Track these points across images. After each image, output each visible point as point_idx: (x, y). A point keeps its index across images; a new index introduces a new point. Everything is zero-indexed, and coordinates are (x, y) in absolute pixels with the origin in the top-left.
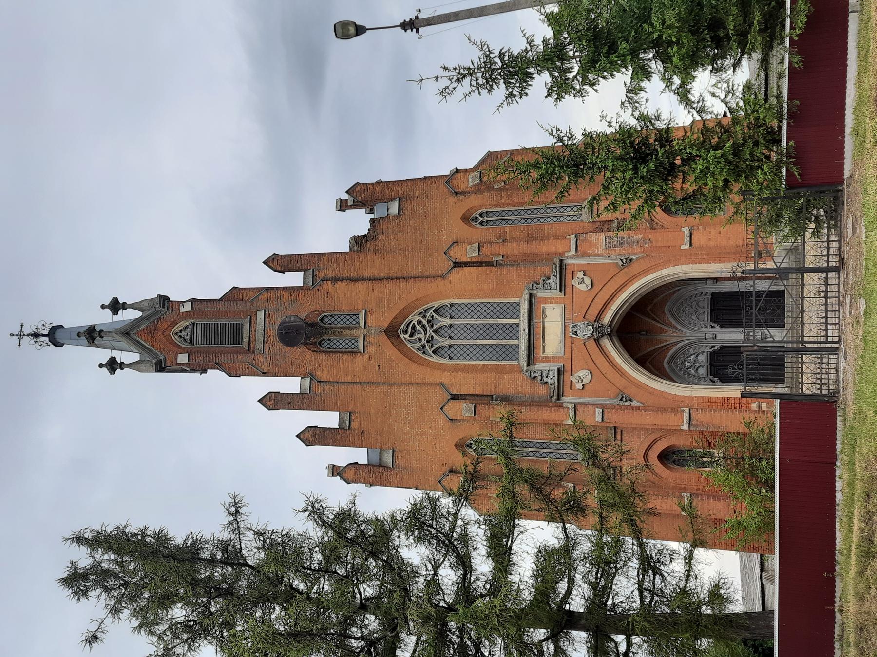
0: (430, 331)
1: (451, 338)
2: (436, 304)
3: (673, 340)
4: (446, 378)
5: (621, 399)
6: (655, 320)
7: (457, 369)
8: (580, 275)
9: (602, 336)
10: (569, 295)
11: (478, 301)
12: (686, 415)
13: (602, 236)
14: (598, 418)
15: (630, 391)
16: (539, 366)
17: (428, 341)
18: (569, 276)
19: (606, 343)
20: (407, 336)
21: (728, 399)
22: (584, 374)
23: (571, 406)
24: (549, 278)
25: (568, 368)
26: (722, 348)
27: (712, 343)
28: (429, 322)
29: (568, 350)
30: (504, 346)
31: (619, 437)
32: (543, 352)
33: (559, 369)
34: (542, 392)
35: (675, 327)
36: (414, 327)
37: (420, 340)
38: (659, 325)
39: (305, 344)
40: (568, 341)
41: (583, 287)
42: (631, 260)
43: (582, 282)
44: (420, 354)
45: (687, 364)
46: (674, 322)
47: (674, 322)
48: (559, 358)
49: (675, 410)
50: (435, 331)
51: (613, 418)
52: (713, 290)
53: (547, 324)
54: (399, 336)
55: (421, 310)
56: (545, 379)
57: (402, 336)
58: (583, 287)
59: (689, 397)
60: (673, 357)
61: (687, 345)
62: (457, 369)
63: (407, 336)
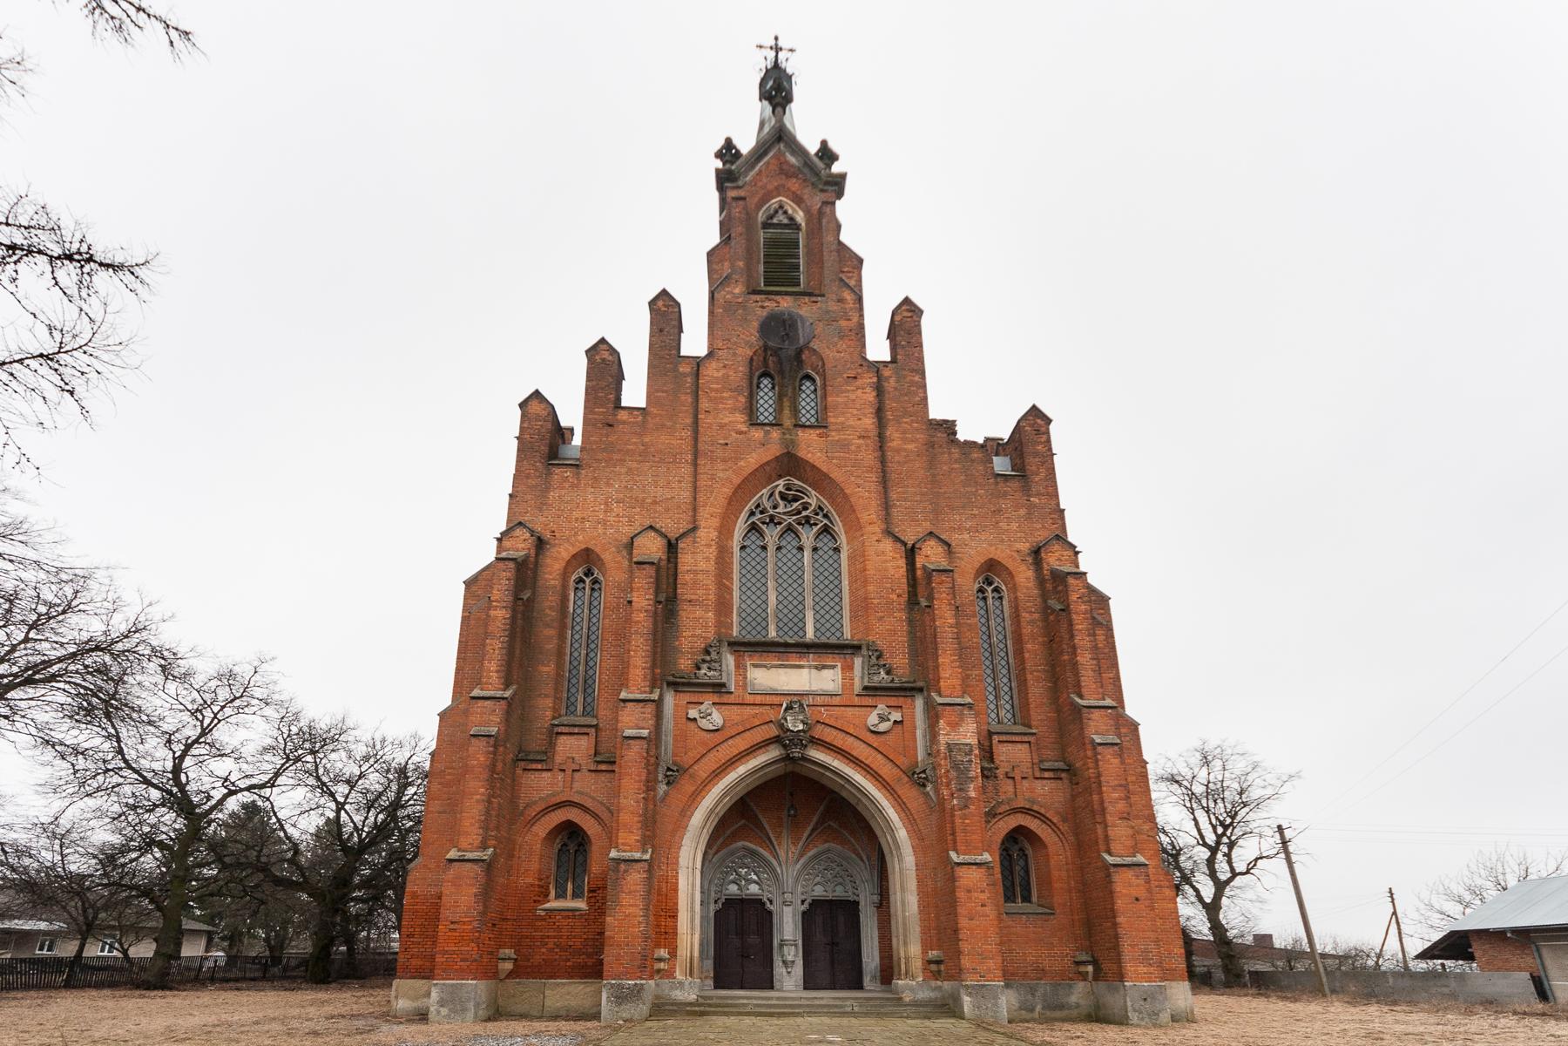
0: (791, 519)
1: (779, 548)
2: (839, 527)
3: (782, 854)
4: (708, 532)
5: (669, 769)
6: (813, 830)
7: (723, 554)
8: (896, 716)
10: (857, 701)
11: (845, 583)
15: (687, 787)
16: (729, 660)
17: (772, 518)
18: (893, 701)
19: (774, 753)
20: (780, 488)
21: (675, 917)
22: (717, 718)
23: (655, 696)
24: (888, 673)
25: (725, 699)
27: (777, 901)
28: (807, 519)
29: (758, 699)
31: (603, 767)
32: (755, 666)
33: (723, 685)
34: (685, 664)
36: (796, 499)
37: (775, 507)
39: (766, 348)
40: (776, 700)
42: (924, 786)
43: (882, 719)
44: (751, 505)
46: (811, 853)
47: (811, 853)
49: (648, 840)
50: (790, 528)
51: (633, 756)
53: (806, 671)
54: (780, 477)
55: (828, 507)
57: (781, 482)
59: (677, 863)
61: (774, 870)
62: (723, 554)
63: (780, 488)
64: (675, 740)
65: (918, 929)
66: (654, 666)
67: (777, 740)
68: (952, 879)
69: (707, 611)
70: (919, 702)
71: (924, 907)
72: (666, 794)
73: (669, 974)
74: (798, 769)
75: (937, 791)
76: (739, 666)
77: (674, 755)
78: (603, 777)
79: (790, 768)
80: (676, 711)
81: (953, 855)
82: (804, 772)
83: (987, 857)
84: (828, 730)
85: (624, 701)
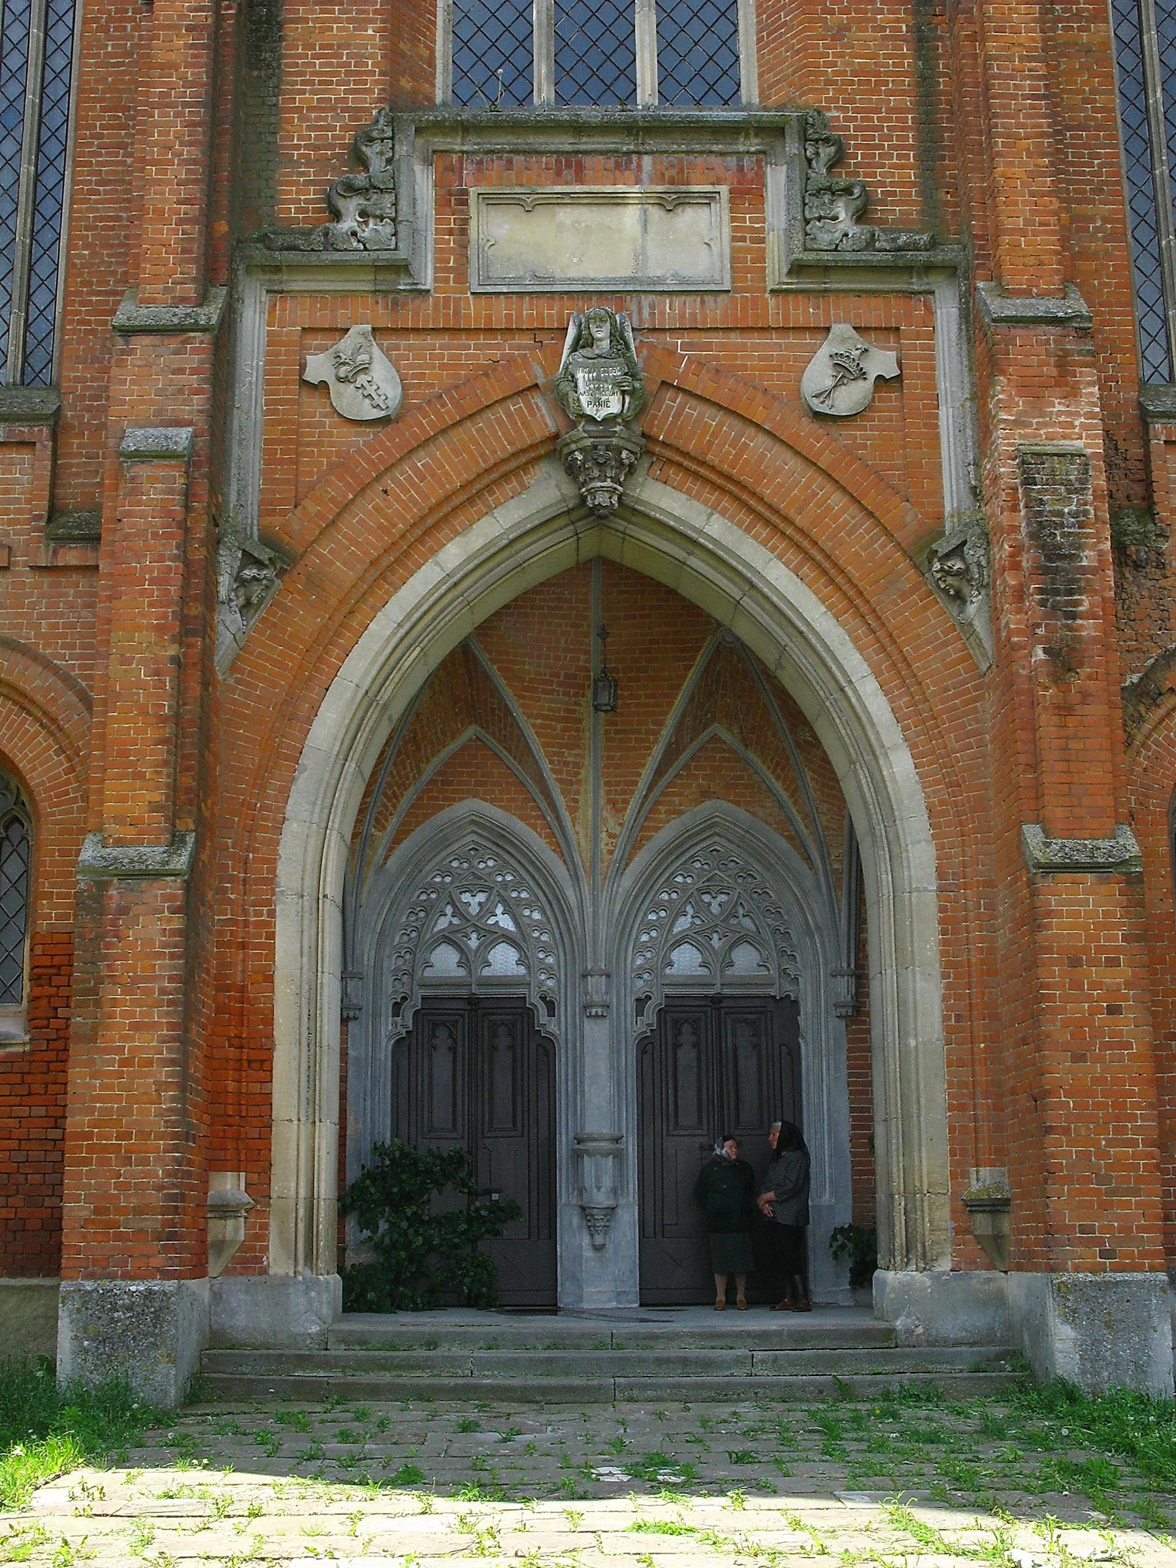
8: (882, 362)
9: (572, 470)
12: (154, 854)
13: (1089, 443)
14: (136, 439)
18: (875, 312)
19: (545, 491)
21: (264, 1064)
24: (861, 216)
26: (546, 1048)
29: (501, 313)
30: (525, 43)
32: (492, 200)
33: (402, 268)
34: (296, 199)
35: (637, 845)
38: (647, 772)
40: (550, 313)
41: (817, 375)
42: (959, 598)
43: (846, 371)
45: (473, 901)
48: (461, 275)
52: (806, 1007)
56: (351, 207)
58: (817, 375)
59: (271, 882)
60: (501, 840)
64: (270, 459)
65: (941, 1096)
66: (208, 218)
67: (552, 448)
68: (1032, 919)
69: (361, 24)
70: (946, 312)
71: (958, 1023)
72: (244, 648)
73: (250, 1260)
74: (612, 548)
75: (994, 615)
76: (453, 200)
77: (267, 507)
78: (73, 589)
79: (591, 544)
80: (272, 361)
81: (1033, 834)
82: (630, 559)
83: (1129, 843)
84: (694, 410)
85: (128, 332)
